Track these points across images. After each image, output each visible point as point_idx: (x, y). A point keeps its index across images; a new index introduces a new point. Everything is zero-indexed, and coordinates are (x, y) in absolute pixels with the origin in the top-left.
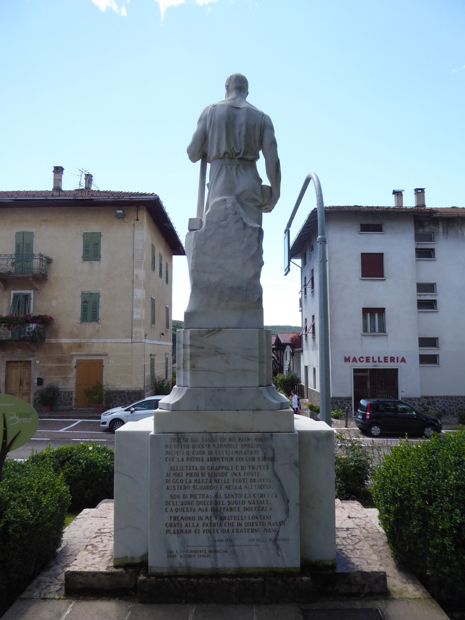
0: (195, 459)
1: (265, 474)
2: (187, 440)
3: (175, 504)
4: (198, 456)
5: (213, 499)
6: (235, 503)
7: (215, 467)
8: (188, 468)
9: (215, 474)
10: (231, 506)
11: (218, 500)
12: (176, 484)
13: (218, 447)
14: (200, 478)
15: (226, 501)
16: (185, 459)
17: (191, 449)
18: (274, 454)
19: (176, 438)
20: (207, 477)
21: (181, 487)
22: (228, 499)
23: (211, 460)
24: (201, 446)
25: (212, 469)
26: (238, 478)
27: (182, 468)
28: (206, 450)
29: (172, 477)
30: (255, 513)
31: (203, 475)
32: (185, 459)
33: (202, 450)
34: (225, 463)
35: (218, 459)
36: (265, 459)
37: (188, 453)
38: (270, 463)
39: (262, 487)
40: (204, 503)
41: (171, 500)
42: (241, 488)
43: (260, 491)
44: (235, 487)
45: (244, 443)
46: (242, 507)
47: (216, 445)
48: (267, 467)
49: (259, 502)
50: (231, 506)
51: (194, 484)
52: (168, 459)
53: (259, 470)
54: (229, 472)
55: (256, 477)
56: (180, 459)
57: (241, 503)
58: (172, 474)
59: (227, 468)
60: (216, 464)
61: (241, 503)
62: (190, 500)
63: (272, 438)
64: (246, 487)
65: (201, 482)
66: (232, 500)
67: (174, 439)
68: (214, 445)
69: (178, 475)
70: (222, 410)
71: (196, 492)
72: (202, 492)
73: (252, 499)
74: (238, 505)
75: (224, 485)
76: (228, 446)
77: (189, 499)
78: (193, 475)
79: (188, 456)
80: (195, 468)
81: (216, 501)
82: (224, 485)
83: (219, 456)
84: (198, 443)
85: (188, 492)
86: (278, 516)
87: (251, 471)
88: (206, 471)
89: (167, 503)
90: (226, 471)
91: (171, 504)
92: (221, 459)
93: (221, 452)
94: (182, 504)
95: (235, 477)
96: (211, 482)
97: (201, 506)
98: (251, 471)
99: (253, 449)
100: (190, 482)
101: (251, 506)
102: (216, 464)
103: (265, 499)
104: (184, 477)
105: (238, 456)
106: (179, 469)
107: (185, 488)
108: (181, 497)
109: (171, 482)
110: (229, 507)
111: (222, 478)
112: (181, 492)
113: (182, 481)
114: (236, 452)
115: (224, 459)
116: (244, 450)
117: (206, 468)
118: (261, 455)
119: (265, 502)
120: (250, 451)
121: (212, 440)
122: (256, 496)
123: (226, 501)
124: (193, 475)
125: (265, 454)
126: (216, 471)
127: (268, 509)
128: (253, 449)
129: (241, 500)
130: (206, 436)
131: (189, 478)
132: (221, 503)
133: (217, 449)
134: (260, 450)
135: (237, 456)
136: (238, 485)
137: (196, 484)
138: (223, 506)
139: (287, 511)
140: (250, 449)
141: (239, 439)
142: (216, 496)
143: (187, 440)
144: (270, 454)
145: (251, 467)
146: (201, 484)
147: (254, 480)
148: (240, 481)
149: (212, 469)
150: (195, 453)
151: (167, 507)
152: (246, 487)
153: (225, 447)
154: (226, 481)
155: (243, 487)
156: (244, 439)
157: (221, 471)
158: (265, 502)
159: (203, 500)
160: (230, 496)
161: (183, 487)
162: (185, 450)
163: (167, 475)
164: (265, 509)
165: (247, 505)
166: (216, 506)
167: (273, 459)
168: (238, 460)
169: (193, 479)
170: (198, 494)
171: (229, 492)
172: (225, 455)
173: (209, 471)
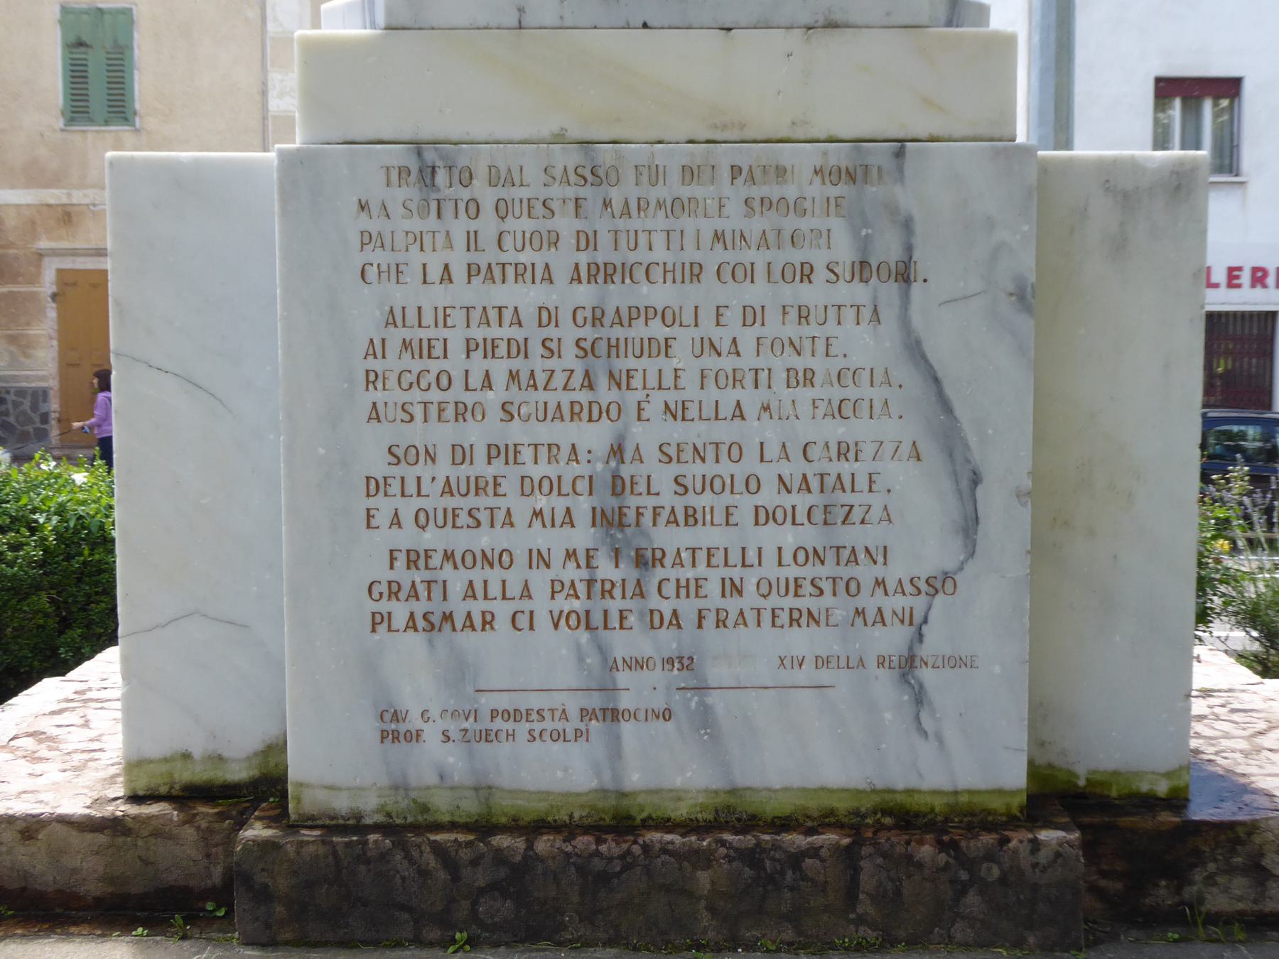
0: (510, 271)
1: (865, 346)
2: (467, 178)
3: (411, 488)
4: (525, 257)
5: (599, 466)
6: (708, 484)
7: (610, 313)
8: (476, 315)
9: (613, 348)
10: (691, 499)
11: (626, 471)
12: (416, 395)
13: (626, 212)
14: (538, 363)
15: (663, 477)
16: (459, 272)
17: (488, 225)
18: (909, 249)
19: (414, 166)
20: (570, 357)
21: (441, 410)
22: (674, 469)
23: (592, 278)
24: (539, 209)
25: (597, 319)
26: (727, 363)
27: (442, 317)
28: (566, 225)
29: (393, 363)
30: (810, 536)
31: (550, 349)
32: (459, 272)
33: (545, 225)
34: (658, 294)
35: (628, 272)
36: (862, 269)
37: (472, 241)
38: (889, 291)
39: (847, 410)
40: (554, 486)
41: (396, 471)
42: (739, 412)
43: (837, 431)
44: (708, 411)
45: (757, 192)
46: (745, 504)
47: (617, 206)
48: (875, 311)
49: (830, 481)
50: (691, 499)
51: (504, 396)
52: (372, 273)
53: (831, 328)
54: (684, 338)
55: (818, 364)
56: (435, 273)
57: (740, 486)
58: (394, 346)
59: (667, 316)
60: (618, 296)
61: (740, 486)
62: (489, 471)
63: (900, 170)
64: (766, 408)
65: (540, 384)
66: (695, 470)
67: (404, 172)
68: (607, 204)
69: (426, 350)
70: (645, 26)
71: (517, 432)
72: (546, 432)
73: (793, 469)
74: (727, 498)
75: (658, 398)
76: (677, 206)
77: (481, 468)
78: (502, 350)
79: (473, 257)
80: (507, 315)
81: (616, 477)
82: (658, 398)
83: (632, 257)
84: (524, 193)
85: (475, 434)
86: (922, 542)
87: (791, 330)
88: (568, 333)
89: (375, 486)
90: (667, 332)
91: (395, 488)
92: (640, 274)
93: (643, 239)
94: (448, 489)
95: (710, 361)
96: (589, 384)
97: (542, 502)
98: (791, 330)
99: (805, 224)
100: (488, 383)
101: (788, 500)
102: (618, 296)
103: (861, 469)
104: (456, 363)
105: (730, 257)
106: (428, 319)
107: (462, 412)
108: (444, 456)
109: (392, 382)
110: (679, 503)
111: (644, 362)
112: (443, 435)
113: (443, 381)
114: (718, 237)
115: (657, 273)
116: (756, 226)
117: (565, 316)
118: (844, 251)
119: (862, 483)
120: (786, 236)
121: (595, 176)
122: (814, 452)
123: (663, 477)
124: (502, 350)
125: (865, 244)
126: (618, 332)
127: (876, 512)
128: (805, 224)
129: (740, 471)
130: (567, 158)
131: (478, 364)
132: (642, 488)
133: (621, 224)
134: (839, 228)
135: (720, 255)
136: (728, 398)
137: (515, 395)
138: (650, 502)
139: (969, 527)
140: (790, 223)
141: (736, 171)
142: (617, 451)
143: (467, 178)
144: (888, 249)
145: (793, 314)
146: (541, 396)
147: (808, 378)
148: (737, 381)
149: (597, 319)
150: (508, 242)
151: (371, 503)
152: (766, 408)
153: (661, 213)
154: (668, 380)
155: (750, 410)
156: (758, 173)
157: (639, 331)
158: (862, 483)
159: (552, 471)
160: (688, 454)
161: (450, 412)
162: (460, 228)
163: (371, 352)
164: (857, 515)
165: (769, 496)
166: (613, 502)
167: (904, 275)
168: (727, 275)
169: (500, 369)
170: (526, 440)
171: (676, 432)
172: (660, 254)
173: (581, 333)
